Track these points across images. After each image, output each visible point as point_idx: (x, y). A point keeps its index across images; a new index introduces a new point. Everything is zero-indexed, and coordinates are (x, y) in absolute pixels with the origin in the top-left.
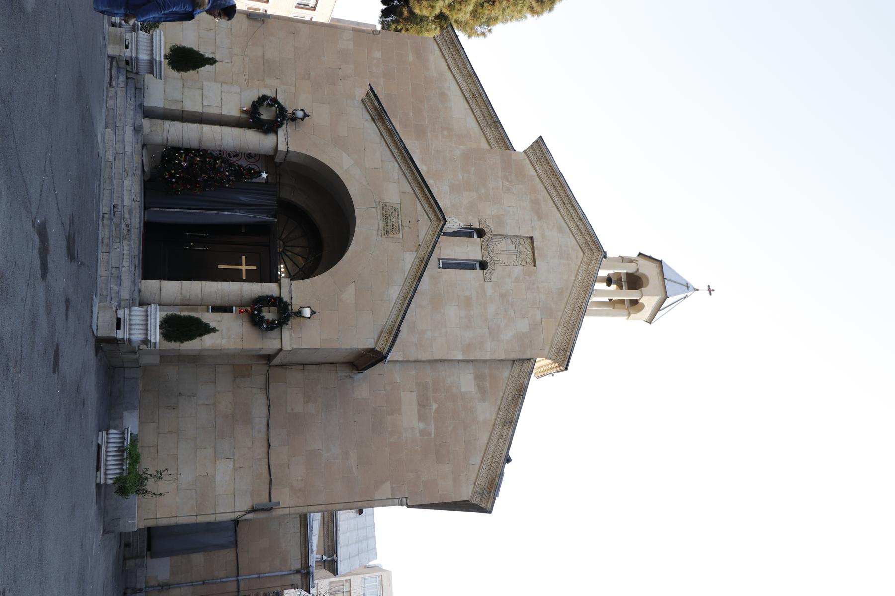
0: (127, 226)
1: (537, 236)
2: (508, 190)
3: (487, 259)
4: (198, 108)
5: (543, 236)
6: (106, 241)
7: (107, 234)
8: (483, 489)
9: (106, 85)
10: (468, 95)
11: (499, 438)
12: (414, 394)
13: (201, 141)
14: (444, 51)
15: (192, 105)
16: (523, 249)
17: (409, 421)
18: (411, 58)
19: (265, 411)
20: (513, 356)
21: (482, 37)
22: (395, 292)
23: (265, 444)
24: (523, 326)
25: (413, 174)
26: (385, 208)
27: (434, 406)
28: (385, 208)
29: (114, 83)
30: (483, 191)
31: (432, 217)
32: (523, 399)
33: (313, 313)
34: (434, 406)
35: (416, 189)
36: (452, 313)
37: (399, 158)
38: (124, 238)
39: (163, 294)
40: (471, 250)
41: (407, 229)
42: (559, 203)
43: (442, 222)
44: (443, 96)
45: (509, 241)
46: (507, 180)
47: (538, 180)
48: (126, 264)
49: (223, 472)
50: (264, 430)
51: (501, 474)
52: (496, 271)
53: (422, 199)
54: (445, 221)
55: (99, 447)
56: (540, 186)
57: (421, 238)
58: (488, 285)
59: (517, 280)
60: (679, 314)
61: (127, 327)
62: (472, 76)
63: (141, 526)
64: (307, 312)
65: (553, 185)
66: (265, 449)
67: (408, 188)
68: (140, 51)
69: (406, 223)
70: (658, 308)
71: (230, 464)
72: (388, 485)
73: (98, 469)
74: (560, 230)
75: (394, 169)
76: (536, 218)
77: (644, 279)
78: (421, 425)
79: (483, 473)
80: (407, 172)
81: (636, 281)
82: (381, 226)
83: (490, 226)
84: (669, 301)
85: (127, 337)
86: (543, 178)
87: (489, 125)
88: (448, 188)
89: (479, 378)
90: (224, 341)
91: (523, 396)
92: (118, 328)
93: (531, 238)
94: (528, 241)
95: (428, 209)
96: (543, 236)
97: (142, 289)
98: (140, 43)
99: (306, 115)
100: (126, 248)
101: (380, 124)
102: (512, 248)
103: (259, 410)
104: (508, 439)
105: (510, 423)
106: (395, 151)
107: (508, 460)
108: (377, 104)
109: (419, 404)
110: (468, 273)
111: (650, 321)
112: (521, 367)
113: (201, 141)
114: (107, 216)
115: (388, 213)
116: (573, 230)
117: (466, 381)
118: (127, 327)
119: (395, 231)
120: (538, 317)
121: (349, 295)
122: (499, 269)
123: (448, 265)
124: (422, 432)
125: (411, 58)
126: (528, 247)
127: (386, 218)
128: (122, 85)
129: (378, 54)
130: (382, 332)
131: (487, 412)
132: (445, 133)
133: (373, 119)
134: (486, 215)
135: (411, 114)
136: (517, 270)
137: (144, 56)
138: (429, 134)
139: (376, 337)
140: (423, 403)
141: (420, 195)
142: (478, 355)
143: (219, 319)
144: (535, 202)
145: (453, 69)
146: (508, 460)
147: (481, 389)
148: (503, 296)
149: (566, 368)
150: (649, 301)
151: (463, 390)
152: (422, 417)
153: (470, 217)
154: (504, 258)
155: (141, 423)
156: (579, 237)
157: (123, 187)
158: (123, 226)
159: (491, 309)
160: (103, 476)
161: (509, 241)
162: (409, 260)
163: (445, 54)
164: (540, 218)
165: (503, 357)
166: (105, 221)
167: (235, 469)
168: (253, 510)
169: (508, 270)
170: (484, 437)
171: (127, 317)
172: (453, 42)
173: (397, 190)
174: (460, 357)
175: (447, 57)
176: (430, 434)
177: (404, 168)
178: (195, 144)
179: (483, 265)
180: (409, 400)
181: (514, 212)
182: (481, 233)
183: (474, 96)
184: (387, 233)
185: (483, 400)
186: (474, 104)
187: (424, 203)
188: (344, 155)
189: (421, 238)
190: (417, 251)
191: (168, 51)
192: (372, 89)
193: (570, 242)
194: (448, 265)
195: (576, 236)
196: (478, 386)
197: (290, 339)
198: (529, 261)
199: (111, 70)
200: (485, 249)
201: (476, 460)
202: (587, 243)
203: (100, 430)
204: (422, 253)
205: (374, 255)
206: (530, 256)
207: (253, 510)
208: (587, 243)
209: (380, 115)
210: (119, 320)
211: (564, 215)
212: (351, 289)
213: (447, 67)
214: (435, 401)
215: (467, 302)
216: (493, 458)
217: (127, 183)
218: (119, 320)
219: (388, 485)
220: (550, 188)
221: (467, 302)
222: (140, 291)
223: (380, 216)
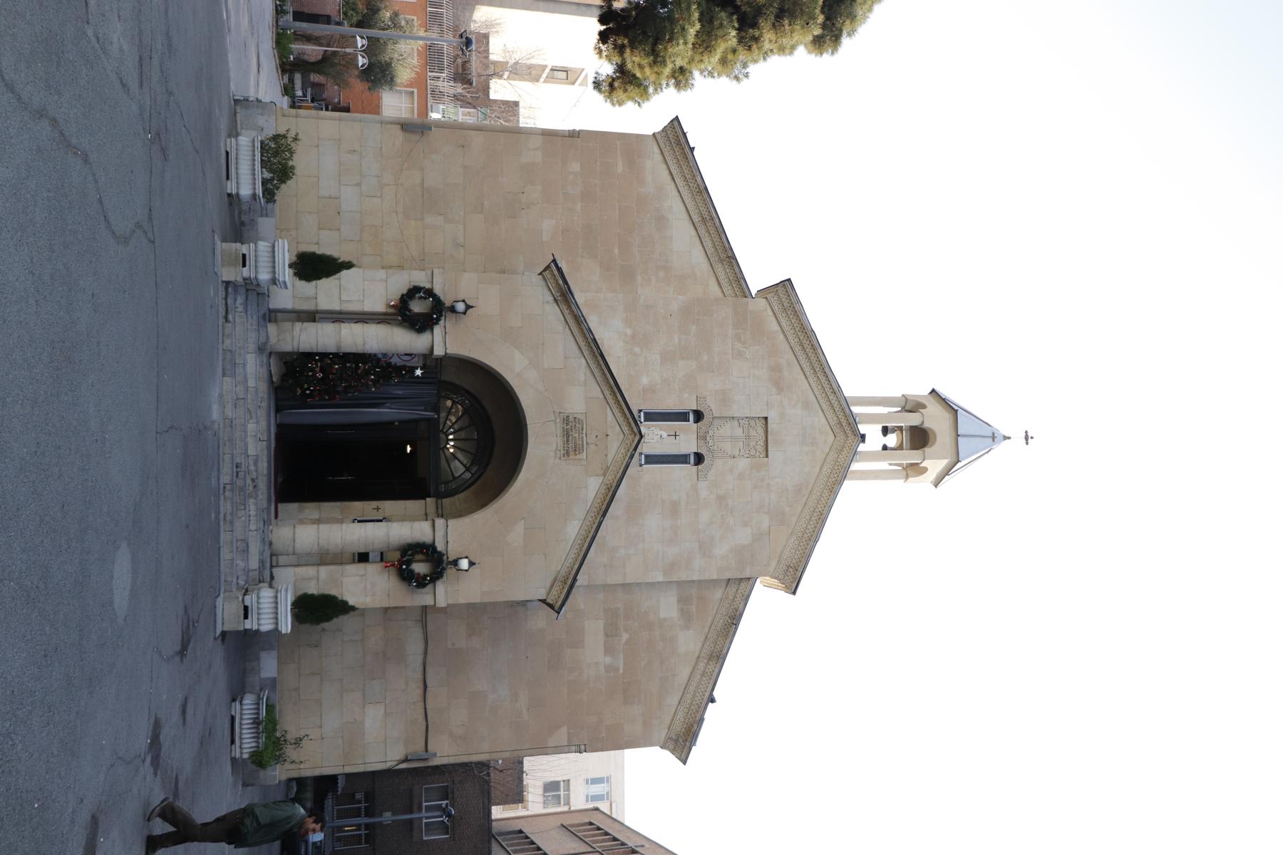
0: (253, 480)
1: (772, 416)
3: (703, 451)
4: (336, 306)
6: (228, 517)
7: (229, 508)
8: (678, 736)
9: (221, 320)
10: (696, 218)
11: (703, 674)
12: (601, 623)
13: (339, 347)
14: (666, 154)
15: (325, 304)
16: (753, 433)
17: (594, 654)
18: (620, 168)
19: (419, 647)
20: (728, 575)
21: (735, 82)
22: (573, 529)
23: (421, 686)
24: (743, 536)
25: (604, 373)
26: (566, 420)
27: (625, 637)
28: (566, 420)
29: (230, 317)
30: (705, 358)
31: (626, 429)
32: (736, 629)
33: (471, 564)
34: (625, 637)
35: (607, 393)
36: (653, 523)
37: (586, 353)
38: (250, 496)
39: (298, 545)
40: (686, 439)
41: (592, 447)
42: (807, 369)
43: (638, 437)
44: (661, 221)
45: (736, 423)
46: (740, 341)
47: (782, 336)
48: (253, 527)
49: (373, 718)
50: (421, 669)
51: (702, 720)
52: (714, 466)
53: (614, 407)
54: (641, 436)
55: (233, 718)
56: (784, 346)
57: (610, 458)
58: (703, 485)
60: (977, 474)
61: (255, 616)
62: (702, 192)
63: (284, 777)
64: (464, 564)
65: (801, 345)
66: (420, 691)
67: (596, 391)
68: (260, 270)
69: (592, 439)
70: (947, 472)
71: (381, 710)
72: (564, 729)
73: (233, 742)
74: (806, 405)
75: (580, 366)
76: (774, 390)
77: (931, 436)
78: (608, 660)
79: (680, 715)
80: (596, 371)
81: (926, 432)
82: (560, 444)
83: (712, 407)
84: (959, 465)
85: (255, 627)
86: (788, 334)
87: (721, 261)
88: (658, 357)
89: (683, 601)
90: (368, 599)
91: (737, 625)
92: (246, 617)
93: (766, 418)
94: (760, 424)
95: (621, 419)
97: (274, 541)
98: (260, 259)
99: (468, 307)
100: (252, 507)
101: (564, 307)
102: (739, 432)
103: (414, 647)
104: (713, 678)
105: (718, 657)
106: (582, 344)
107: (713, 701)
108: (561, 282)
109: (606, 635)
111: (937, 483)
112: (739, 588)
113: (339, 347)
114: (228, 487)
115: (571, 430)
116: (824, 406)
117: (667, 607)
118: (255, 616)
119: (577, 449)
121: (516, 535)
122: (719, 463)
123: (651, 459)
124: (608, 669)
125: (620, 168)
126: (761, 431)
127: (567, 434)
128: (241, 308)
129: (576, 167)
130: (555, 580)
131: (689, 642)
132: (661, 274)
133: (556, 300)
134: (707, 391)
135: (616, 251)
136: (743, 464)
137: (264, 276)
138: (639, 278)
139: (548, 585)
140: (611, 632)
141: (611, 401)
142: (683, 576)
143: (362, 572)
144: (776, 369)
145: (678, 181)
146: (713, 701)
147: (687, 617)
148: (721, 499)
149: (794, 593)
150: (934, 466)
151: (662, 615)
152: (608, 650)
153: (686, 395)
154: (727, 446)
155: (280, 663)
156: (830, 415)
157: (245, 431)
158: (249, 481)
159: (705, 516)
160: (238, 750)
161: (736, 423)
162: (593, 487)
163: (668, 159)
164: (780, 390)
165: (715, 577)
166: (227, 493)
167: (386, 714)
168: (406, 760)
169: (729, 467)
170: (685, 672)
171: (255, 605)
172: (679, 143)
173: (581, 395)
174: (660, 579)
175: (670, 163)
176: (618, 670)
177: (593, 366)
178: (332, 349)
179: (699, 459)
180: (594, 630)
181: (742, 385)
182: (699, 416)
183: (704, 220)
184: (568, 454)
185: (688, 628)
186: (702, 231)
187: (616, 411)
188: (517, 354)
189: (610, 458)
190: (604, 475)
191: (294, 259)
192: (554, 261)
193: (819, 421)
194: (651, 459)
195: (827, 413)
196: (682, 610)
197: (443, 594)
198: (761, 448)
199: (226, 299)
200: (702, 437)
201: (673, 700)
202: (840, 423)
203: (234, 700)
204: (611, 478)
205: (550, 480)
206: (762, 443)
207: (406, 760)
208: (840, 423)
209: (564, 295)
210: (246, 608)
211: (814, 385)
212: (520, 528)
213: (669, 178)
214: (626, 631)
215: (674, 509)
216: (694, 695)
217: (251, 427)
218: (246, 608)
219: (564, 729)
220: (798, 349)
221: (674, 509)
222: (271, 543)
223: (559, 432)
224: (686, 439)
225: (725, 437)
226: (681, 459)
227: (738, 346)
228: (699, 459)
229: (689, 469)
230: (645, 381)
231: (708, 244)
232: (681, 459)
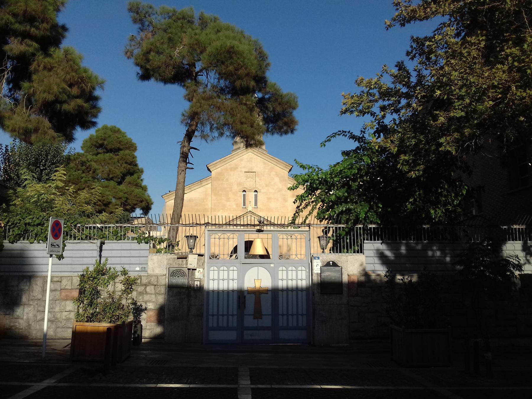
2: (227, 180)
5: (244, 167)
10: (189, 191)
24: (277, 180)
40: (251, 196)
58: (262, 191)
59: (260, 180)
74: (241, 160)
87: (201, 184)
96: (244, 167)
110: (259, 198)
120: (274, 173)
148: (266, 186)
156: (244, 154)
159: (271, 191)
164: (237, 168)
186: (193, 189)
200: (250, 190)
221: (269, 199)
224: (251, 196)
225: (249, 184)
226: (256, 196)
227: (225, 180)
228: (256, 191)
229: (259, 194)
230: (234, 206)
231: (197, 187)
232: (256, 196)
